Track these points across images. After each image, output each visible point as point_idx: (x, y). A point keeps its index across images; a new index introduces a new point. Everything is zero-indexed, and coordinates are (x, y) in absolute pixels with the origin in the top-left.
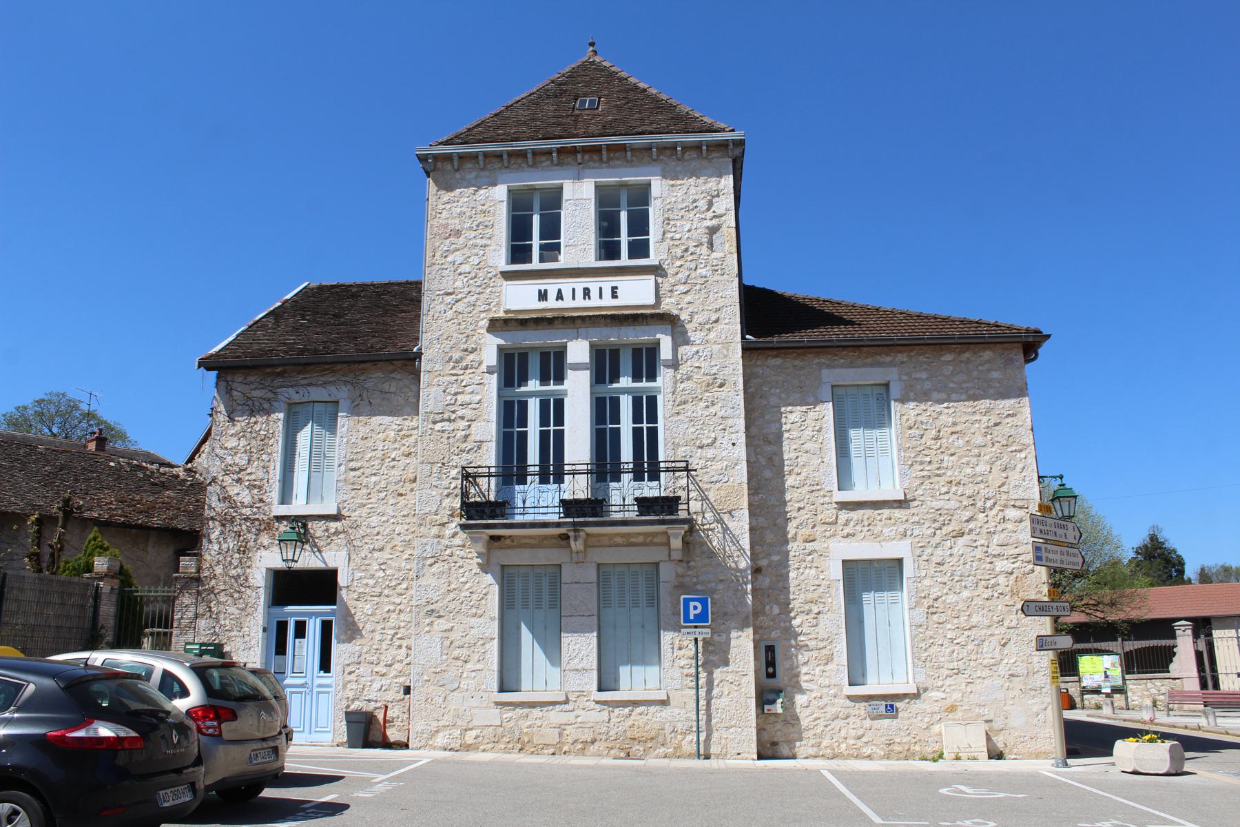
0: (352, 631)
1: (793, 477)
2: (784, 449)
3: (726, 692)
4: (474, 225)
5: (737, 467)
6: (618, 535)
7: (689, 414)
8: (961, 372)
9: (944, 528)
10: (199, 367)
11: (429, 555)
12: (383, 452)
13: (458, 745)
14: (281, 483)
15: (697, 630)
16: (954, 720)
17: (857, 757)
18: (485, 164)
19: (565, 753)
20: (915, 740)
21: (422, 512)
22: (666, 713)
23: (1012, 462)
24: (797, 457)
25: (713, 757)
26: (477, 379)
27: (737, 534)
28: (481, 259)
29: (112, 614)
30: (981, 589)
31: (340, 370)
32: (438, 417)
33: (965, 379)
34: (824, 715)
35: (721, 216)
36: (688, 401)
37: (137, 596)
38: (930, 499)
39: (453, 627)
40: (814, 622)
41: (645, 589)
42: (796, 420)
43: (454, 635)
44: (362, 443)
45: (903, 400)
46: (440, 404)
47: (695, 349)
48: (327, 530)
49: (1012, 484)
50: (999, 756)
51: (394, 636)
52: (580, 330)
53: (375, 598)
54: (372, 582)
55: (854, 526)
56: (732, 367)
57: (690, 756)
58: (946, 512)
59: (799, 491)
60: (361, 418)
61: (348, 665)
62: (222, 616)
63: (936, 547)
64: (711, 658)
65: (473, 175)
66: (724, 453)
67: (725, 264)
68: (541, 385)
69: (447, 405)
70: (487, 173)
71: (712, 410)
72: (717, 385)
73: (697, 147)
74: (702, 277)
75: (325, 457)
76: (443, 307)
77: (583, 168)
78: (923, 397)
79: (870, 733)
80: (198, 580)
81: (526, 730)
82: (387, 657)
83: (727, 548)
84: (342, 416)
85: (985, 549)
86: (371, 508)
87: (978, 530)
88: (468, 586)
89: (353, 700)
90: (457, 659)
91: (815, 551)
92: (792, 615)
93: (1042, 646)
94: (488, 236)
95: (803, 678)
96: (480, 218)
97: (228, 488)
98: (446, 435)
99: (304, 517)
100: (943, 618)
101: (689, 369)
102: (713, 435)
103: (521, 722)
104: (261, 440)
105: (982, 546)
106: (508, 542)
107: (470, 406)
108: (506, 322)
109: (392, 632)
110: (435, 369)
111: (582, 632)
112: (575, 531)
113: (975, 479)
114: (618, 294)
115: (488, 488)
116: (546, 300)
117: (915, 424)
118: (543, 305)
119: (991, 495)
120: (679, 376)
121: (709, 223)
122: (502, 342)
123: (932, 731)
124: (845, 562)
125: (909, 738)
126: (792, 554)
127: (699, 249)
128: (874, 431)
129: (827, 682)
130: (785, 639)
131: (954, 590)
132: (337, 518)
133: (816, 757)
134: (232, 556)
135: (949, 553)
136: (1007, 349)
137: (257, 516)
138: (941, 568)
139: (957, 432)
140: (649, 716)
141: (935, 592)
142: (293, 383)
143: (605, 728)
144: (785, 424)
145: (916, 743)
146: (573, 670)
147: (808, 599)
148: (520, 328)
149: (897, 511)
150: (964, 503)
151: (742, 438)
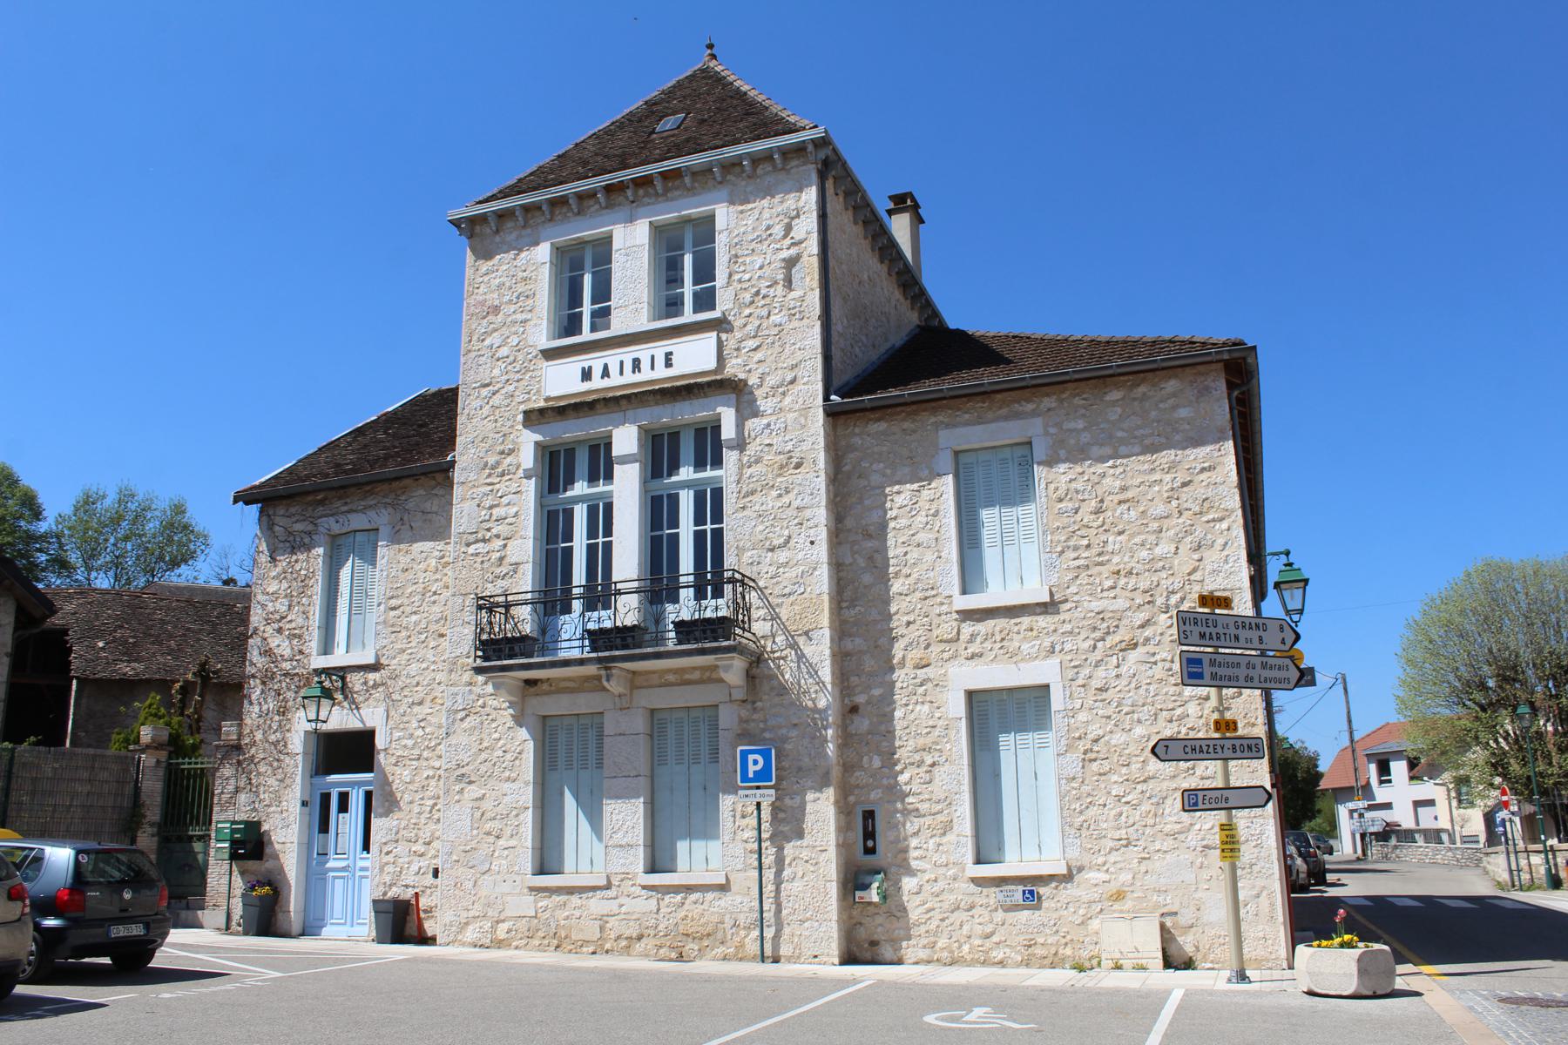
0: (392, 804)
1: (901, 580)
2: (889, 543)
3: (800, 874)
5: (817, 573)
6: (669, 671)
7: (757, 508)
8: (1133, 414)
9: (1109, 638)
10: (236, 501)
11: (460, 708)
12: (423, 586)
13: (488, 941)
14: (323, 631)
15: (758, 792)
16: (1121, 911)
17: (984, 963)
18: (526, 222)
19: (607, 952)
20: (1064, 941)
21: (453, 655)
22: (726, 901)
23: (1209, 536)
24: (906, 554)
25: (783, 960)
26: (514, 487)
27: (815, 662)
29: (160, 790)
30: (1161, 723)
32: (472, 538)
33: (1139, 423)
34: (939, 905)
35: (801, 242)
36: (756, 491)
37: (184, 770)
38: (1087, 598)
39: (484, 795)
40: (927, 777)
41: (707, 740)
42: (905, 502)
43: (487, 805)
44: (402, 576)
45: (1050, 463)
46: (474, 522)
47: (765, 421)
48: (365, 683)
49: (1209, 568)
50: (1188, 965)
51: (433, 807)
52: (627, 412)
53: (414, 763)
54: (410, 743)
55: (982, 643)
56: (811, 440)
57: (754, 959)
58: (1111, 615)
59: (908, 599)
60: (402, 546)
61: (385, 844)
62: (262, 789)
63: (1096, 666)
64: (781, 828)
65: (513, 236)
66: (800, 556)
68: (589, 487)
70: (529, 231)
71: (786, 499)
72: (792, 466)
73: (767, 157)
74: (775, 326)
75: (367, 596)
77: (637, 206)
78: (1078, 455)
79: (1002, 930)
80: (238, 748)
81: (563, 922)
82: (425, 835)
83: (803, 681)
84: (382, 546)
85: (1168, 665)
86: (411, 654)
87: (1158, 638)
88: (502, 742)
89: (390, 885)
90: (489, 834)
91: (929, 680)
92: (898, 768)
93: (1196, 804)
94: (528, 308)
95: (913, 854)
96: (520, 288)
97: (269, 640)
98: (479, 559)
99: (342, 669)
100: (1106, 766)
102: (786, 533)
103: (558, 912)
104: (302, 581)
105: (1164, 660)
106: (545, 687)
107: (506, 521)
108: (542, 412)
109: (431, 802)
111: (627, 798)
112: (607, 668)
113: (1152, 566)
114: (673, 362)
115: (525, 620)
117: (1067, 494)
118: (587, 386)
119: (1177, 586)
120: (745, 459)
121: (785, 254)
122: (539, 438)
123: (1090, 927)
124: (971, 695)
125: (1056, 938)
126: (898, 685)
127: (772, 290)
128: (1014, 509)
129: (944, 860)
130: (888, 802)
131: (1121, 727)
132: (375, 667)
133: (929, 962)
134: (271, 719)
135: (1114, 674)
136: (1200, 374)
137: (297, 671)
138: (1104, 696)
139: (1128, 501)
140: (705, 906)
141: (1095, 730)
142: (334, 511)
143: (653, 921)
144: (891, 509)
145: (1066, 944)
146: (617, 846)
147: (919, 747)
148: (559, 418)
149: (1040, 618)
150: (1137, 601)
151: (822, 535)
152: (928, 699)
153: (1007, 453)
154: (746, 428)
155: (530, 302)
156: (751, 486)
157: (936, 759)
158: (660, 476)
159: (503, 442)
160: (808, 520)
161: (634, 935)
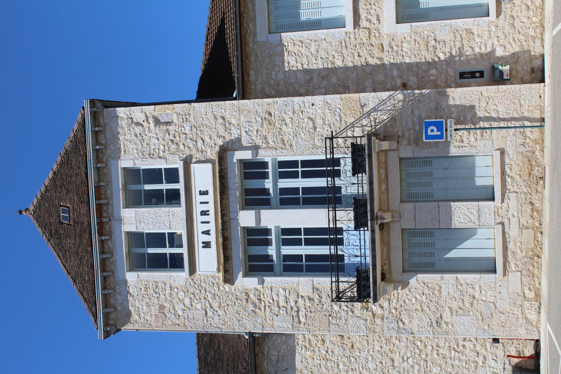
1: (336, 61)
2: (315, 68)
3: (494, 107)
5: (329, 101)
7: (291, 138)
11: (396, 325)
12: (322, 360)
13: (536, 303)
15: (449, 129)
17: (543, 9)
18: (111, 289)
19: (541, 225)
21: (365, 330)
22: (510, 151)
24: (322, 58)
25: (542, 116)
26: (268, 292)
32: (296, 319)
34: (511, 35)
35: (147, 116)
39: (449, 308)
40: (442, 43)
42: (294, 59)
43: (455, 305)
47: (244, 134)
51: (456, 351)
52: (231, 217)
53: (429, 364)
54: (416, 367)
56: (257, 107)
57: (542, 133)
59: (346, 56)
64: (469, 119)
66: (319, 111)
67: (181, 113)
68: (272, 245)
69: (287, 313)
70: (117, 287)
71: (288, 121)
72: (270, 118)
73: (96, 134)
74: (192, 130)
76: (216, 318)
81: (524, 253)
82: (472, 356)
83: (388, 108)
86: (363, 368)
90: (472, 304)
91: (390, 44)
92: (436, 60)
95: (483, 50)
98: (309, 314)
101: (259, 138)
102: (306, 120)
106: (386, 268)
107: (288, 296)
108: (226, 271)
109: (453, 352)
111: (451, 213)
112: (377, 219)
114: (205, 190)
116: (210, 242)
118: (213, 245)
120: (264, 145)
121: (152, 125)
122: (241, 274)
126: (392, 61)
127: (171, 132)
129: (486, 33)
130: (455, 65)
133: (542, 40)
140: (513, 163)
143: (522, 195)
144: (297, 67)
146: (479, 219)
148: (230, 261)
152: (400, 44)
153: (272, 7)
157: (432, 39)
158: (269, 200)
159: (241, 300)
160: (300, 107)
161: (530, 207)
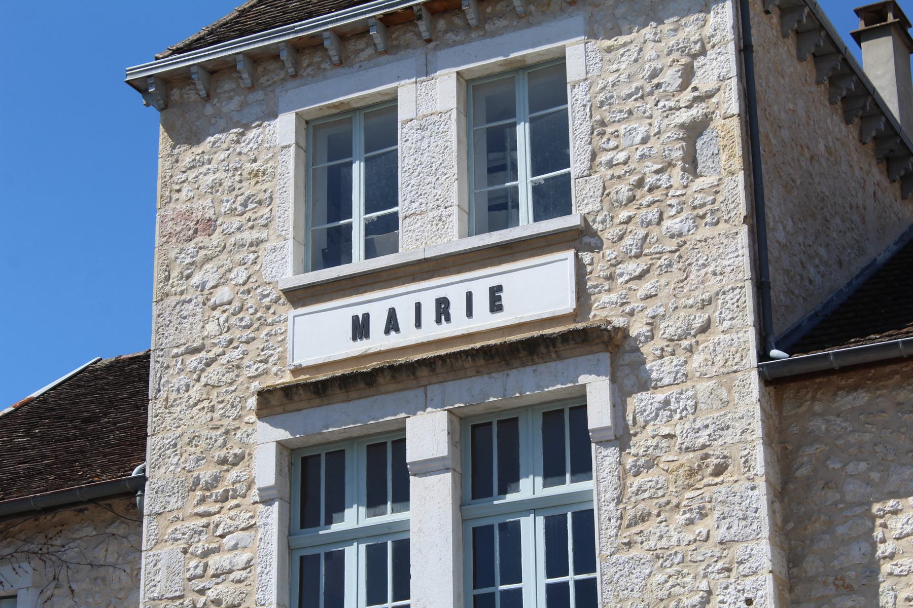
4: (237, 205)
7: (652, 543)
26: (243, 518)
28: (251, 271)
31: (20, 531)
35: (709, 95)
36: (649, 514)
47: (660, 396)
56: (740, 426)
65: (236, 101)
67: (720, 198)
68: (369, 515)
69: (190, 580)
70: (259, 95)
71: (701, 528)
72: (709, 470)
74: (672, 237)
76: (182, 380)
77: (436, 48)
94: (263, 221)
96: (248, 189)
101: (649, 443)
102: (704, 585)
107: (232, 576)
108: (288, 391)
110: (169, 508)
114: (504, 302)
116: (367, 336)
120: (629, 461)
121: (684, 116)
122: (283, 435)
127: (665, 177)
144: (883, 541)
148: (317, 401)
154: (630, 409)
155: (265, 211)
156: (641, 506)
158: (489, 494)
159: (225, 444)
160: (740, 563)
